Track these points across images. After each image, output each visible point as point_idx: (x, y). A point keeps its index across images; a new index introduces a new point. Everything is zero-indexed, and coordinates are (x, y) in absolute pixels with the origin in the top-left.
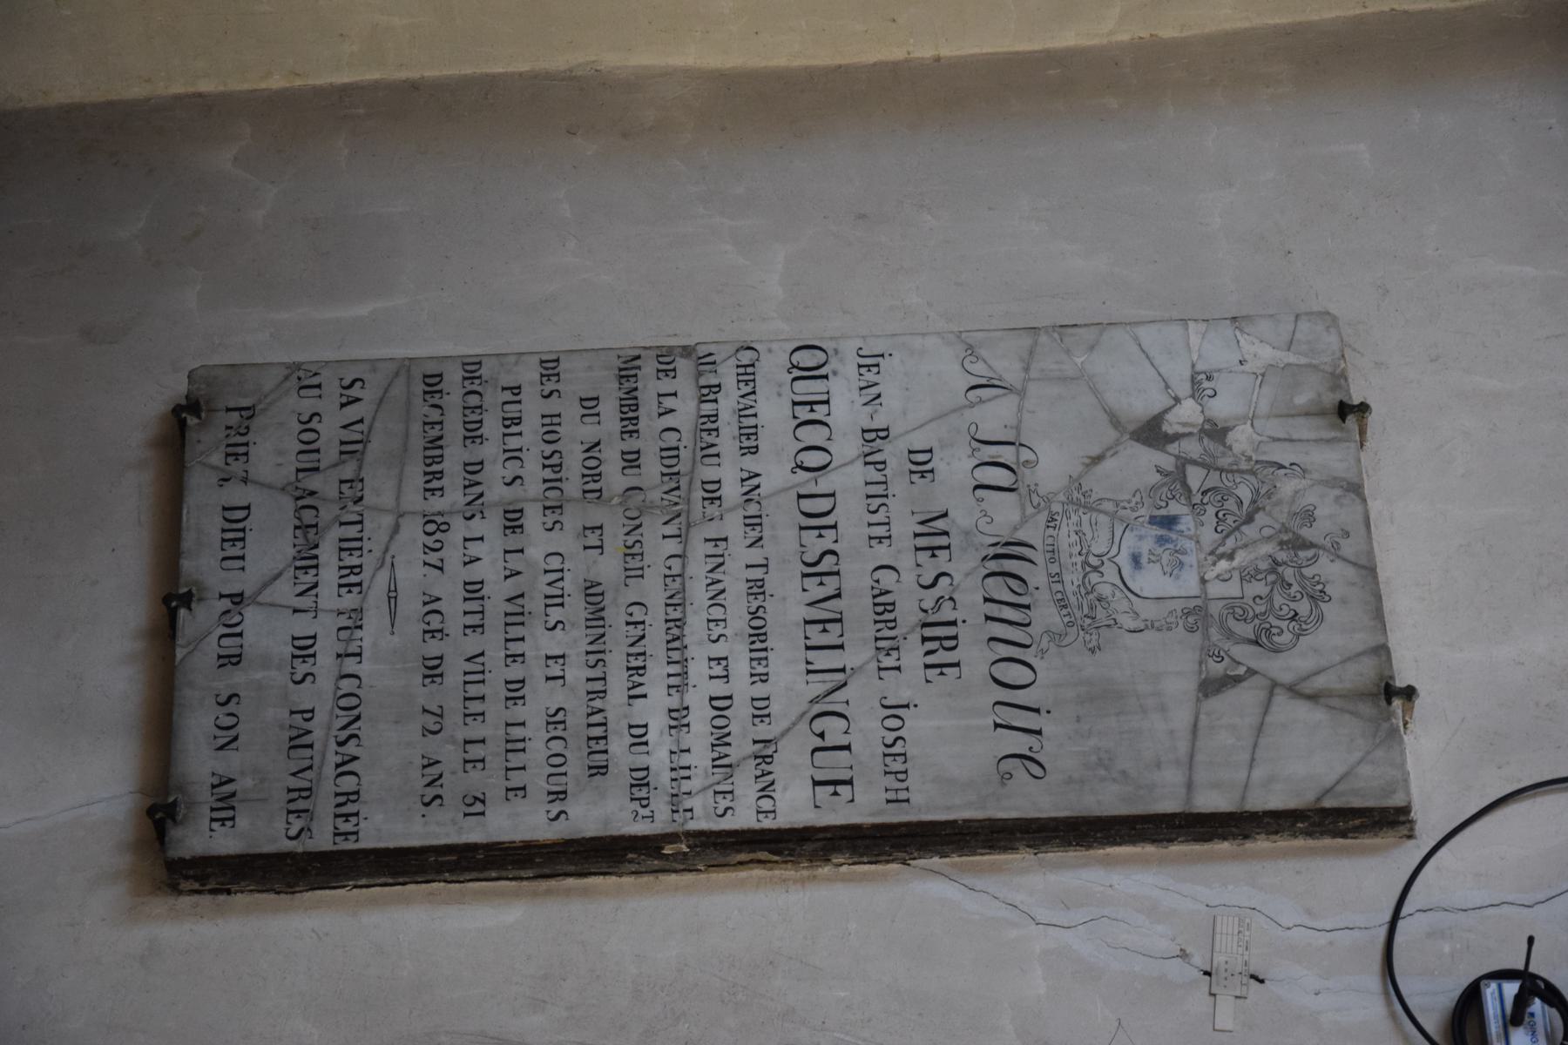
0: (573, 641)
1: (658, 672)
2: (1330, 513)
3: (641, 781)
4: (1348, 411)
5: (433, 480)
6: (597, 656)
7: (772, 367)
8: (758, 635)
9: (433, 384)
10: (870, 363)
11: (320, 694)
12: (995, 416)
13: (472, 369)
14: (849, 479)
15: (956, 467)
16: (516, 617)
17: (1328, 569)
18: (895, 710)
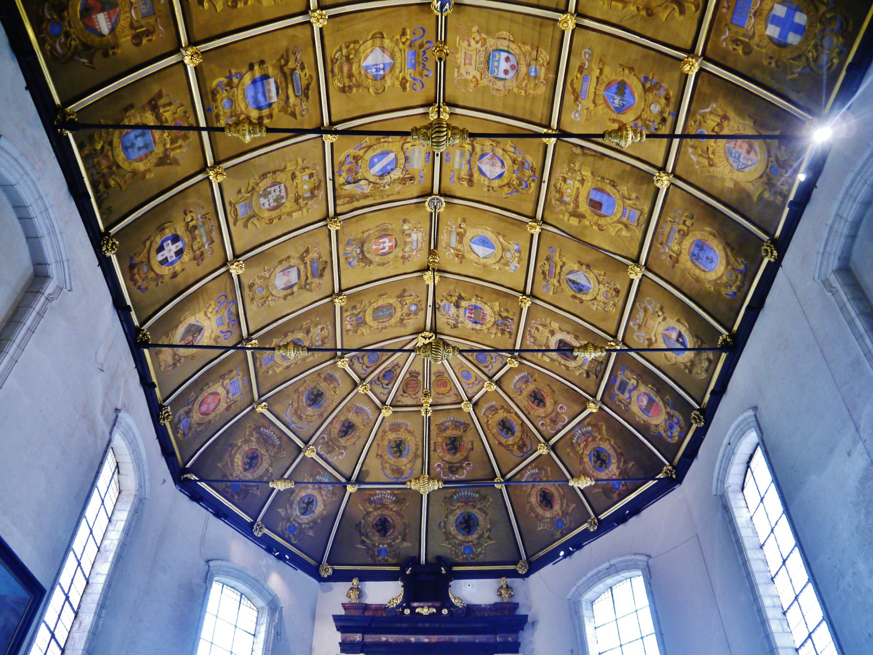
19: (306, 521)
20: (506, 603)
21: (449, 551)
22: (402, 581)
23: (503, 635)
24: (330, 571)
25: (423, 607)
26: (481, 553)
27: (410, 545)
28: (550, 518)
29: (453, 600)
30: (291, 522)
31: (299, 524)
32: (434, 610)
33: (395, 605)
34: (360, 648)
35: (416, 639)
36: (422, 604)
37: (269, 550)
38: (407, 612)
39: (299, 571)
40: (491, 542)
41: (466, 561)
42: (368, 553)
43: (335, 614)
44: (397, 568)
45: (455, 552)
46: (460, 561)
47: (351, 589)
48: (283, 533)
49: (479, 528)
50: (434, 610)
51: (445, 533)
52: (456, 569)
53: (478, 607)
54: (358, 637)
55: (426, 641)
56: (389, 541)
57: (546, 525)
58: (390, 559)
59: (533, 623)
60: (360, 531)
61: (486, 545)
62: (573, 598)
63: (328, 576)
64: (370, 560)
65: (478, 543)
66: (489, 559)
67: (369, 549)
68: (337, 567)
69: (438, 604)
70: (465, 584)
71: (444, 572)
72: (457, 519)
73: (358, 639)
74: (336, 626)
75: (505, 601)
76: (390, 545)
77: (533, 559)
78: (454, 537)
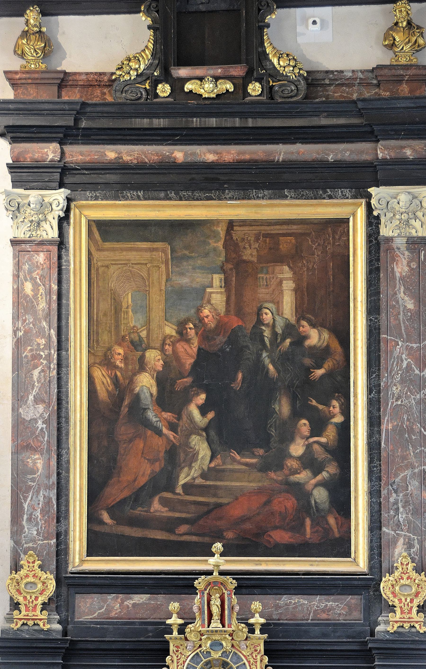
20: (406, 67)
22: (148, 12)
23: (393, 143)
25: (201, 79)
29: (275, 61)
32: (229, 86)
33: (134, 74)
34: (57, 176)
35: (186, 155)
36: (199, 71)
47: (25, 34)
55: (211, 157)
70: (305, 20)
73: (51, 156)
75: (403, 61)
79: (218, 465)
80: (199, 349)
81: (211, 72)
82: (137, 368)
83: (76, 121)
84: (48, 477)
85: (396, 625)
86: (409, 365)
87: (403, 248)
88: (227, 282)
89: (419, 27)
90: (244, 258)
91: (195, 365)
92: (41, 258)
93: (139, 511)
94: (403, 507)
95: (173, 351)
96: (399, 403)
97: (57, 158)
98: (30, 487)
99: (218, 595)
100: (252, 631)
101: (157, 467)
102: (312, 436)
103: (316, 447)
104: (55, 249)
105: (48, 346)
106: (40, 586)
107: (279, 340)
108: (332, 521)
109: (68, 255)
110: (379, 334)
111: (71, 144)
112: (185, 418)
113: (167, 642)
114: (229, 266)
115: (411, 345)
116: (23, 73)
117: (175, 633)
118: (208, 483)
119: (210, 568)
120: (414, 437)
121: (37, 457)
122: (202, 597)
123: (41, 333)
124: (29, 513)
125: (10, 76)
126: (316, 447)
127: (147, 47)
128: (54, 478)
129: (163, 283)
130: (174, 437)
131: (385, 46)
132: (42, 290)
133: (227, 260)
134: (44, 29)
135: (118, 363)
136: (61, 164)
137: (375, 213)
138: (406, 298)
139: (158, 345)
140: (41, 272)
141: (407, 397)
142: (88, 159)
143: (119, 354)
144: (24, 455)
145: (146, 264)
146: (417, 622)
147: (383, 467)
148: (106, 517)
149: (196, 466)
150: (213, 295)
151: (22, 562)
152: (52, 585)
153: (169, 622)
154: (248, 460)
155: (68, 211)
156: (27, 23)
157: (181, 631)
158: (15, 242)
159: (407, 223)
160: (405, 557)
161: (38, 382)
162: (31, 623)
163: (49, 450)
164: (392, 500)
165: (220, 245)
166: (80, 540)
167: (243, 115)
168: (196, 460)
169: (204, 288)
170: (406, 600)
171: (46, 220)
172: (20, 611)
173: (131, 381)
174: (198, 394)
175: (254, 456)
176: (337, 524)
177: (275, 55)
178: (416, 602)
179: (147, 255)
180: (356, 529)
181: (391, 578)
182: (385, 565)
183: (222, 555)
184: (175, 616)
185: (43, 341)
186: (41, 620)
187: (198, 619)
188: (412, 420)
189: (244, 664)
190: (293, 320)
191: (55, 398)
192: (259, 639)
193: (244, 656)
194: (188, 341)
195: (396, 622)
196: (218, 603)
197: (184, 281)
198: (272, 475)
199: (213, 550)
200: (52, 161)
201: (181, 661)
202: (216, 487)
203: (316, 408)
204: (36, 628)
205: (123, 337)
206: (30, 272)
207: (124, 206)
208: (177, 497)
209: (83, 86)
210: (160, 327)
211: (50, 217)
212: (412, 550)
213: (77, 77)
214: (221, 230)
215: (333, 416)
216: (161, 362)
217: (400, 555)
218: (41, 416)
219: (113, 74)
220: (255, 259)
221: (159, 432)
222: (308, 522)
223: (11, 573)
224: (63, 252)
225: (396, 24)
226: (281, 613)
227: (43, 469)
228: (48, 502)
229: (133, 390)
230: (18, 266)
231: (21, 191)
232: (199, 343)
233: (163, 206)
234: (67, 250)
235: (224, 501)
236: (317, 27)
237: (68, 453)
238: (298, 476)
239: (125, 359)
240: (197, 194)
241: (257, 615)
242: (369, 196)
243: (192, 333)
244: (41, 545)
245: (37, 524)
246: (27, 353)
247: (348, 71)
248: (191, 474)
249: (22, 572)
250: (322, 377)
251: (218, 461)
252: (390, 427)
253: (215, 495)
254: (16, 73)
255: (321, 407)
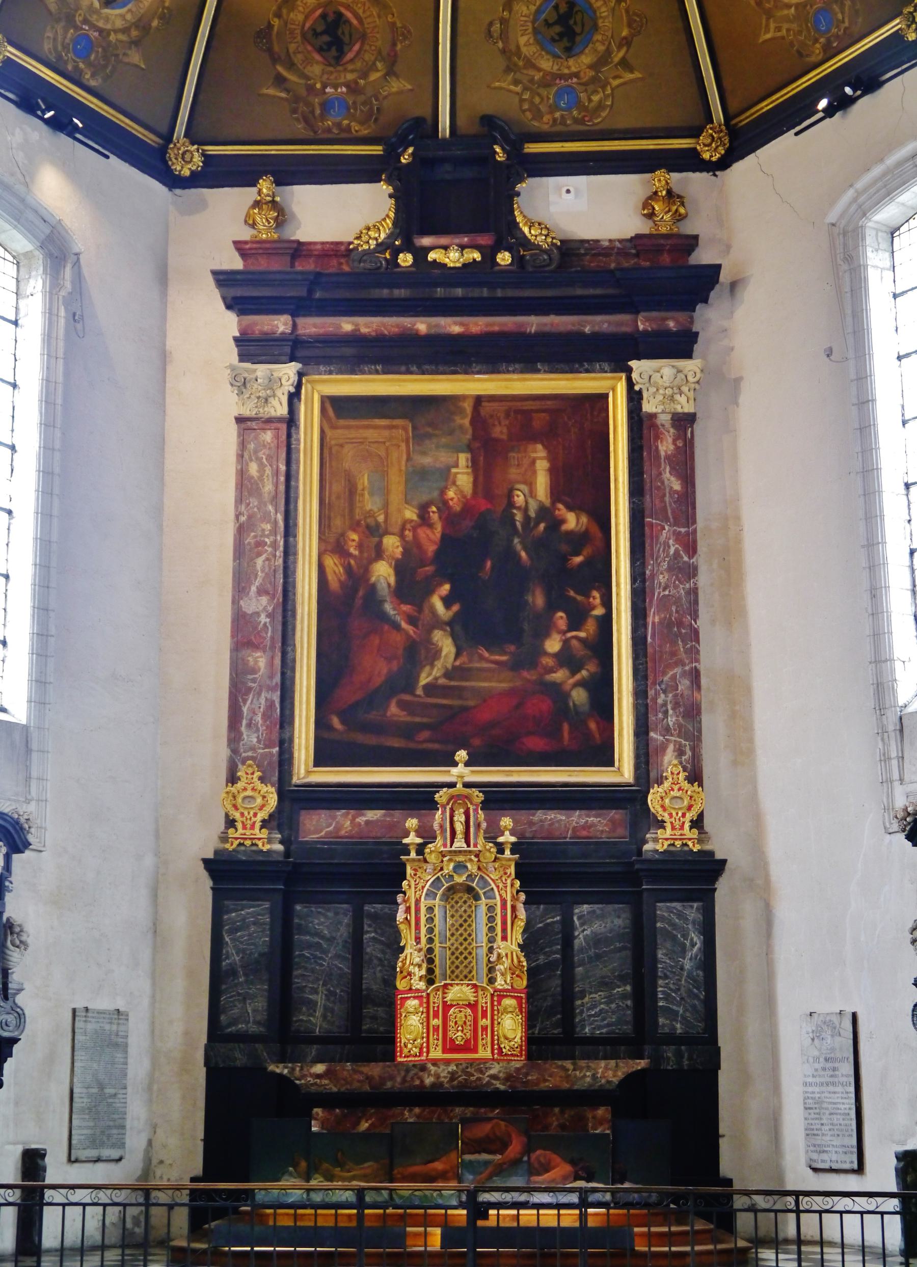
0: (835, 1116)
1: (838, 1106)
2: (821, 1018)
3: (850, 1109)
4: (811, 1014)
5: (817, 1135)
6: (836, 1114)
7: (807, 1089)
8: (835, 1093)
9: (808, 1135)
10: (805, 1076)
11: (840, 1150)
12: (811, 1060)
13: (806, 1129)
14: (818, 1080)
15: (817, 1066)
16: (832, 1124)
17: (828, 1019)
18: (842, 1075)
19: (119, 24)
21: (517, 99)
22: (389, 182)
23: (654, 314)
24: (198, 160)
25: (446, 248)
26: (600, 106)
27: (409, 87)
28: (797, 6)
29: (526, 230)
30: (76, 28)
31: (101, 31)
32: (477, 256)
33: (373, 243)
34: (288, 350)
35: (429, 326)
36: (443, 241)
37: (27, 105)
38: (406, 260)
39: (113, 159)
40: (629, 76)
41: (559, 128)
42: (294, 111)
43: (217, 267)
44: (377, 150)
45: (532, 103)
46: (545, 128)
47: (257, 204)
48: (59, 57)
49: (598, 37)
50: (477, 256)
51: (503, 51)
52: (533, 148)
53: (592, 247)
54: (281, 324)
55: (456, 329)
56: (350, 77)
57: (785, 26)
58: (355, 126)
59: (733, 286)
60: (270, 50)
61: (615, 83)
62: (843, 222)
63: (192, 172)
64: (300, 129)
65: (594, 80)
66: (623, 123)
67: (297, 99)
68: (212, 150)
69: (485, 240)
70: (558, 189)
71: (501, 156)
72: (538, 12)
73: (281, 328)
74: (224, 299)
75: (663, 230)
76: (353, 88)
77: (745, 119)
78: (530, 64)
79: (464, 663)
80: (444, 537)
81: (457, 241)
82: (373, 556)
83: (310, 292)
84: (271, 677)
85: (666, 843)
86: (677, 552)
87: (668, 425)
88: (474, 464)
89: (679, 197)
90: (494, 435)
91: (438, 553)
92: (268, 436)
93: (373, 716)
94: (673, 709)
95: (415, 536)
96: (667, 593)
97: (289, 331)
98: (250, 689)
99: (462, 810)
100: (501, 851)
101: (395, 666)
102: (570, 629)
103: (574, 642)
104: (284, 427)
105: (274, 532)
106: (259, 801)
107: (532, 524)
108: (593, 726)
109: (298, 433)
110: (643, 517)
111: (304, 316)
112: (426, 611)
113: (404, 865)
114: (477, 445)
115: (679, 529)
116: (253, 242)
117: (413, 855)
118: (453, 683)
119: (453, 779)
120: (683, 631)
121: (258, 654)
122: (444, 812)
123: (266, 517)
124: (249, 717)
125: (239, 246)
126: (574, 642)
127: (388, 216)
128: (278, 679)
129: (403, 463)
130: (414, 632)
131: (644, 215)
132: (268, 471)
133: (475, 437)
134: (278, 199)
135: (352, 550)
136: (292, 337)
137: (637, 388)
138: (673, 479)
139: (396, 529)
140: (267, 452)
141: (676, 587)
142: (322, 331)
143: (353, 540)
144: (245, 652)
145: (384, 443)
146: (690, 839)
147: (649, 664)
148: (336, 722)
149: (439, 664)
150: (459, 476)
151: (239, 774)
152: (273, 800)
153: (405, 841)
154: (497, 658)
155: (299, 386)
156: (260, 192)
157: (420, 849)
158: (240, 420)
159: (672, 398)
160: (675, 766)
161: (262, 571)
162: (248, 843)
163: (273, 647)
164: (660, 701)
165: (466, 422)
166: (307, 748)
167: (492, 286)
168: (440, 657)
169: (448, 469)
170: (677, 814)
171: (274, 396)
172: (236, 830)
173: (367, 570)
174: (441, 585)
175: (504, 653)
176: (598, 728)
177: (525, 224)
178: (689, 816)
179: (386, 433)
180: (621, 734)
181: (660, 790)
182: (653, 775)
183: (467, 764)
184: (412, 834)
185: (268, 527)
186: (259, 839)
187: (439, 838)
188: (681, 612)
189: (492, 889)
190: (547, 502)
191: (280, 589)
192: (510, 860)
193: (493, 880)
194: (431, 526)
195: (667, 839)
196: (463, 819)
197: (427, 461)
198: (525, 674)
199: (457, 758)
200: (283, 333)
201: (420, 886)
202: (461, 689)
203: (574, 599)
204: (254, 848)
205: (358, 523)
206: (256, 452)
207: (361, 381)
208: (416, 699)
209: (319, 256)
210: (400, 511)
211: (279, 393)
212: (683, 758)
213: (312, 247)
214: (468, 406)
215: (594, 608)
216: (401, 549)
217: (670, 763)
218: (265, 609)
219: (351, 243)
220: (504, 437)
221: (397, 627)
222: (566, 727)
223: (227, 785)
224: (293, 430)
225: (656, 193)
226: (535, 831)
227: (265, 668)
228: (270, 705)
229: (368, 580)
230: (242, 445)
231: (248, 365)
232: (444, 528)
233: (404, 381)
234: (298, 427)
235: (471, 703)
236: (570, 197)
237: (294, 650)
238: (554, 675)
239: (360, 546)
240: (441, 368)
241: (507, 833)
242: (629, 370)
243: (435, 517)
244: (262, 754)
245: (258, 730)
246: (250, 540)
247: (605, 240)
248: (434, 673)
249: (240, 785)
250: (581, 565)
251: (464, 659)
252: (657, 620)
253: (461, 698)
254: (246, 242)
255: (579, 598)
